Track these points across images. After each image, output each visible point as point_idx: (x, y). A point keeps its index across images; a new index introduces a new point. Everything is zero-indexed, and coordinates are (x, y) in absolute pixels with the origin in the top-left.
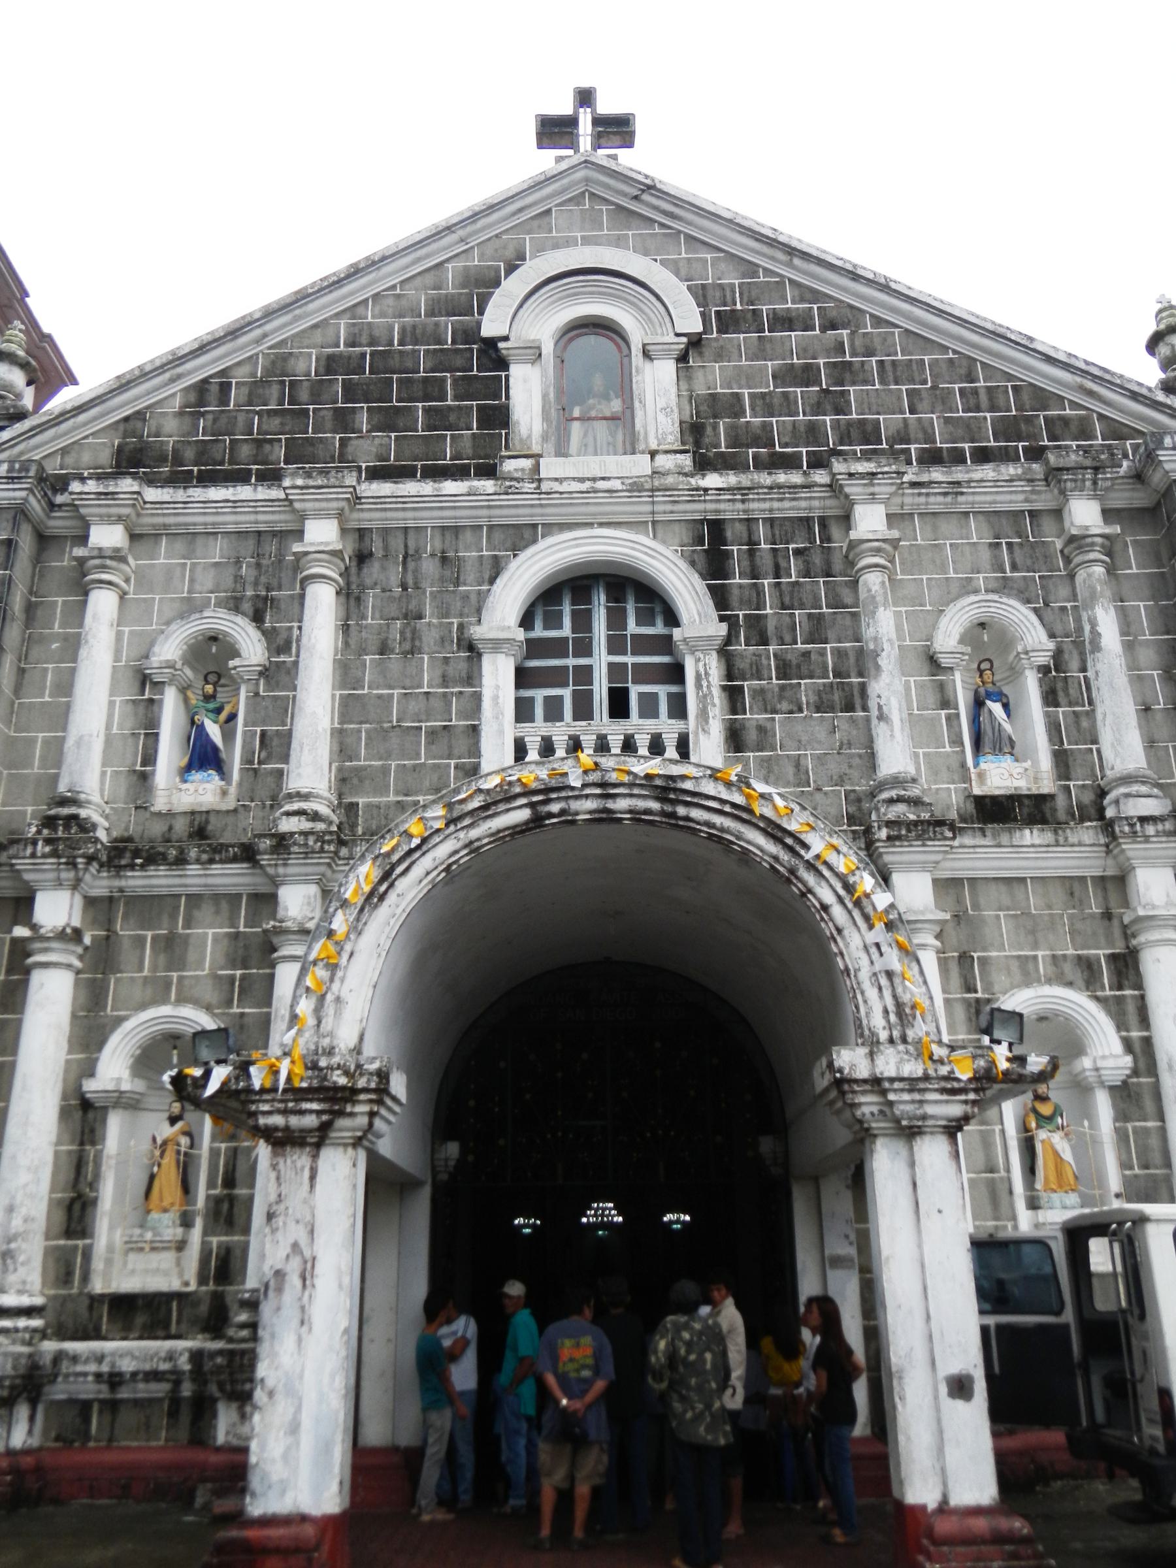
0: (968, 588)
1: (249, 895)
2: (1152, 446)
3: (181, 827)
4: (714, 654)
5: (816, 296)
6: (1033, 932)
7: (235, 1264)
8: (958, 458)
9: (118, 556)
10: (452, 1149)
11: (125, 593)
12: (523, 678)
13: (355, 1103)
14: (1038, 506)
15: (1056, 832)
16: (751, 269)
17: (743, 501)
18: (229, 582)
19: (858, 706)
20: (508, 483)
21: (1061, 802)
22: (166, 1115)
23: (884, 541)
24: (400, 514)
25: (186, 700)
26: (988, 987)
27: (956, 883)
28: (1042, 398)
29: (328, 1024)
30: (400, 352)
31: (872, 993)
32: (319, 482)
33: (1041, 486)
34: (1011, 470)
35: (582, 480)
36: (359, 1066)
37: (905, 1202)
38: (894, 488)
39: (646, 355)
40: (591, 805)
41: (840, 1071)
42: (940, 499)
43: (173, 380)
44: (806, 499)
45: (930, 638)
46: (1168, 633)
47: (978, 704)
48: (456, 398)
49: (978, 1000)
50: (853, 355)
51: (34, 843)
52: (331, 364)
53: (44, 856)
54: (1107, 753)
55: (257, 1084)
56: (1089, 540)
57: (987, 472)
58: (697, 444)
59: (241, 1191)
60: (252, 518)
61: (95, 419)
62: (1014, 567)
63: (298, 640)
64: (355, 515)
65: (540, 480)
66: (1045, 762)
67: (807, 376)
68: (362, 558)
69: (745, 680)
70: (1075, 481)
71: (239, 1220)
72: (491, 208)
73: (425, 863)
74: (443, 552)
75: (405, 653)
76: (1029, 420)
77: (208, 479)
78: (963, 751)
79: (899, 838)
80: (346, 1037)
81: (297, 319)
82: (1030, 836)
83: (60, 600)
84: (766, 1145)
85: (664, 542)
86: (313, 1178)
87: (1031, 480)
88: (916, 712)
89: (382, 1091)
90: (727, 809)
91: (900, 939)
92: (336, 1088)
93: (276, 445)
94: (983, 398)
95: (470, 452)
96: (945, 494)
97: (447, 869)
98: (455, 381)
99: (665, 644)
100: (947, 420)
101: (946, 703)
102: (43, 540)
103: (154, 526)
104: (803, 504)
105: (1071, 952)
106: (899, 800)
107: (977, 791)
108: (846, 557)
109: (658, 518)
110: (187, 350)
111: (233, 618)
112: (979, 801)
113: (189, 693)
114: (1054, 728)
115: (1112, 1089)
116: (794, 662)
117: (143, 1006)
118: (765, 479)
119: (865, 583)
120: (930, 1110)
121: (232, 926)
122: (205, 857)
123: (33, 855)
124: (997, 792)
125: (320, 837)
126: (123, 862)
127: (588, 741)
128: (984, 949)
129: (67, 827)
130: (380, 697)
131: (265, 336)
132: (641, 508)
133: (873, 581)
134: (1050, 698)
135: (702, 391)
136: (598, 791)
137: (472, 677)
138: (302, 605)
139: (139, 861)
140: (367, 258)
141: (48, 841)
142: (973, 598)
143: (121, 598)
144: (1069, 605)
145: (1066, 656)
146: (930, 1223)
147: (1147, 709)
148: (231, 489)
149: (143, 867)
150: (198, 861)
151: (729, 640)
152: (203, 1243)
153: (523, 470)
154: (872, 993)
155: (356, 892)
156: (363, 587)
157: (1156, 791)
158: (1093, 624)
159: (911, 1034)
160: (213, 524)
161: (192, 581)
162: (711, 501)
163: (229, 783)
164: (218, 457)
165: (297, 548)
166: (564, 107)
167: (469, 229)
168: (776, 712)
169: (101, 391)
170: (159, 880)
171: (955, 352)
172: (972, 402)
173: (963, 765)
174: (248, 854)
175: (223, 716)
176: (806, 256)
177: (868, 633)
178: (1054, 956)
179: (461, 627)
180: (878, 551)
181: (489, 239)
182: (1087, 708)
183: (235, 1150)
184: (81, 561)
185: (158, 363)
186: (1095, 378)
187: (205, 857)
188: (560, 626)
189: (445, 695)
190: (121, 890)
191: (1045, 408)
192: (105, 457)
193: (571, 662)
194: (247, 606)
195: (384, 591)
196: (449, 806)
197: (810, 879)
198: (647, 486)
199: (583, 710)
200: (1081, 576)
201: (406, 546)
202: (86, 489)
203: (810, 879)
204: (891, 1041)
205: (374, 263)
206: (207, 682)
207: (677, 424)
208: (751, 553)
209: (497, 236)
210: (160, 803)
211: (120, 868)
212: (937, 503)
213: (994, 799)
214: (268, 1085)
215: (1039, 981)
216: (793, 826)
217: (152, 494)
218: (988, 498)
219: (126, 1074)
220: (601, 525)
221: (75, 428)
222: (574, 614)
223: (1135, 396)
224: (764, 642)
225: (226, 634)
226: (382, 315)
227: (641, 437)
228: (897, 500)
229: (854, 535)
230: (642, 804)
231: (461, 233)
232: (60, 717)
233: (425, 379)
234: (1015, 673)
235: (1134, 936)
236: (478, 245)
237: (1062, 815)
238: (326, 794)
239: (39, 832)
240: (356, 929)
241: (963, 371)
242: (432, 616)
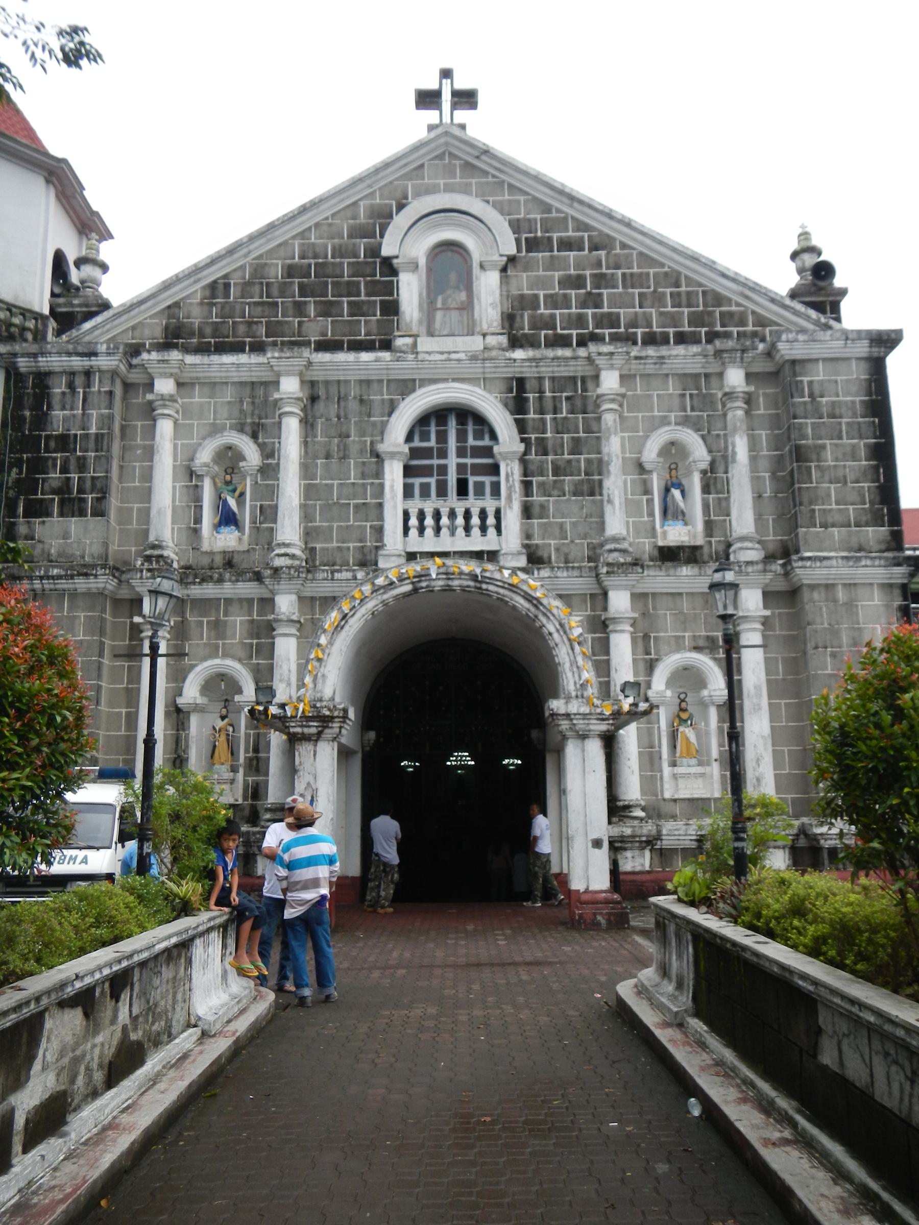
0: (664, 422)
1: (258, 599)
2: (775, 340)
3: (218, 560)
4: (517, 462)
5: (587, 228)
6: (684, 622)
7: (261, 791)
8: (664, 340)
9: (172, 399)
10: (372, 735)
11: (177, 420)
12: (409, 471)
13: (333, 722)
14: (709, 371)
15: (700, 568)
16: (548, 208)
17: (537, 367)
18: (236, 413)
19: (597, 493)
20: (398, 354)
21: (706, 550)
22: (219, 715)
23: (617, 395)
24: (336, 373)
25: (215, 483)
26: (657, 653)
27: (644, 595)
28: (719, 299)
29: (319, 686)
30: (333, 264)
31: (569, 674)
32: (288, 355)
33: (711, 359)
34: (695, 349)
35: (442, 353)
36: (334, 706)
37: (579, 767)
38: (624, 362)
39: (482, 267)
40: (441, 583)
41: (552, 710)
42: (652, 366)
43: (195, 282)
44: (574, 365)
45: (640, 452)
46: (776, 450)
47: (667, 490)
48: (367, 295)
49: (651, 659)
50: (607, 268)
51: (142, 571)
52: (291, 271)
53: (147, 578)
54: (734, 523)
55: (289, 714)
56: (735, 395)
57: (680, 350)
58: (511, 327)
59: (261, 755)
60: (249, 374)
61: (151, 307)
62: (692, 409)
63: (279, 450)
64: (309, 373)
65: (417, 353)
66: (700, 526)
67: (578, 282)
68: (314, 399)
69: (533, 476)
70: (730, 357)
71: (262, 769)
72: (386, 165)
73: (363, 611)
74: (361, 396)
75: (340, 459)
76: (711, 314)
77: (221, 349)
78: (654, 521)
79: (613, 572)
80: (328, 692)
81: (269, 241)
82: (686, 571)
83: (139, 424)
84: (535, 734)
85: (490, 392)
86: (315, 755)
87: (705, 356)
88: (630, 497)
89: (345, 717)
90: (506, 586)
91: (584, 650)
92: (325, 716)
93: (260, 325)
94: (684, 299)
95: (375, 331)
96: (655, 364)
97: (373, 614)
98: (366, 283)
99: (488, 452)
100: (661, 314)
101: (647, 491)
102: (127, 386)
103: (191, 378)
104: (572, 368)
105: (704, 633)
106: (616, 550)
107: (660, 544)
108: (596, 401)
109: (487, 376)
110: (203, 264)
111: (241, 437)
112: (661, 550)
113: (217, 480)
114: (706, 507)
115: (719, 706)
116: (562, 466)
117: (205, 659)
118: (550, 353)
119: (605, 420)
120: (592, 727)
121: (249, 616)
122: (234, 578)
123: (141, 578)
124: (672, 544)
125: (297, 569)
126: (189, 581)
127: (445, 512)
128: (657, 632)
129: (157, 562)
130: (326, 485)
131: (250, 252)
132: (476, 369)
133: (609, 419)
134: (706, 489)
135: (515, 292)
136: (444, 576)
137: (379, 474)
138: (280, 428)
139: (197, 580)
140: (311, 201)
141: (149, 570)
142: (667, 428)
143: (175, 423)
144: (722, 433)
145: (717, 464)
146: (590, 777)
147: (760, 496)
148: (235, 357)
149: (200, 583)
150: (230, 581)
151: (525, 453)
152: (244, 780)
153: (407, 345)
154: (569, 674)
155: (330, 626)
156: (315, 418)
157: (757, 546)
158: (734, 446)
159: (585, 694)
160: (226, 377)
161: (215, 412)
162: (518, 367)
163: (243, 534)
164: (226, 332)
165: (276, 396)
166: (432, 84)
167: (373, 179)
168: (550, 496)
169: (154, 291)
170: (209, 590)
171: (669, 267)
172: (677, 301)
173: (654, 528)
174: (258, 577)
175: (237, 493)
176: (581, 202)
177: (605, 450)
178: (694, 636)
179: (372, 443)
180: (613, 401)
181: (386, 185)
182: (726, 495)
183: (258, 734)
184: (150, 403)
185: (187, 272)
186: (751, 289)
187: (234, 578)
188: (429, 440)
189: (363, 484)
190: (188, 596)
191: (719, 305)
192: (158, 332)
193: (435, 462)
194: (248, 429)
195: (327, 420)
196: (373, 584)
197: (544, 620)
198: (481, 357)
199: (442, 492)
200: (730, 416)
201: (339, 392)
202: (151, 358)
203: (544, 620)
204: (577, 697)
205: (315, 204)
206: (227, 474)
207: (500, 314)
208: (541, 399)
209: (391, 182)
210: (205, 547)
211: (187, 584)
212: (650, 369)
213: (669, 549)
214: (294, 714)
215: (684, 649)
216: (538, 594)
217: (190, 359)
218: (681, 366)
219: (198, 695)
220: (454, 380)
221: (139, 313)
222: (438, 433)
223: (773, 300)
224: (546, 453)
225: (236, 446)
226: (321, 237)
227: (478, 323)
228: (627, 367)
229: (600, 391)
230: (465, 583)
231: (368, 182)
232: (147, 495)
233: (348, 283)
234: (689, 473)
235: (738, 625)
236: (380, 189)
237: (706, 558)
238: (298, 543)
239: (142, 564)
240: (331, 643)
241: (673, 280)
242: (355, 435)
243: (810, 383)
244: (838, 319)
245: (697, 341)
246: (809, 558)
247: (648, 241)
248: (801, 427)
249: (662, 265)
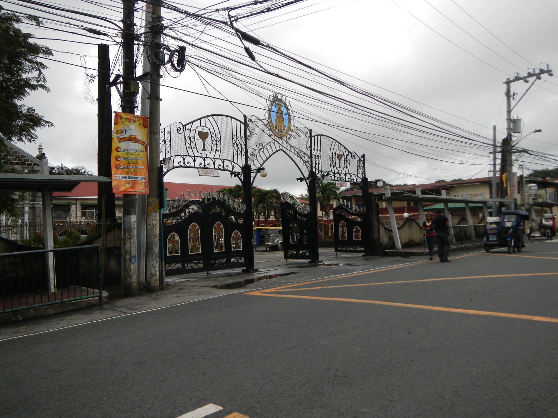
28: (24, 157)
34: (19, 166)
245: (20, 165)
246: (37, 203)
247: (11, 145)
249: (14, 150)
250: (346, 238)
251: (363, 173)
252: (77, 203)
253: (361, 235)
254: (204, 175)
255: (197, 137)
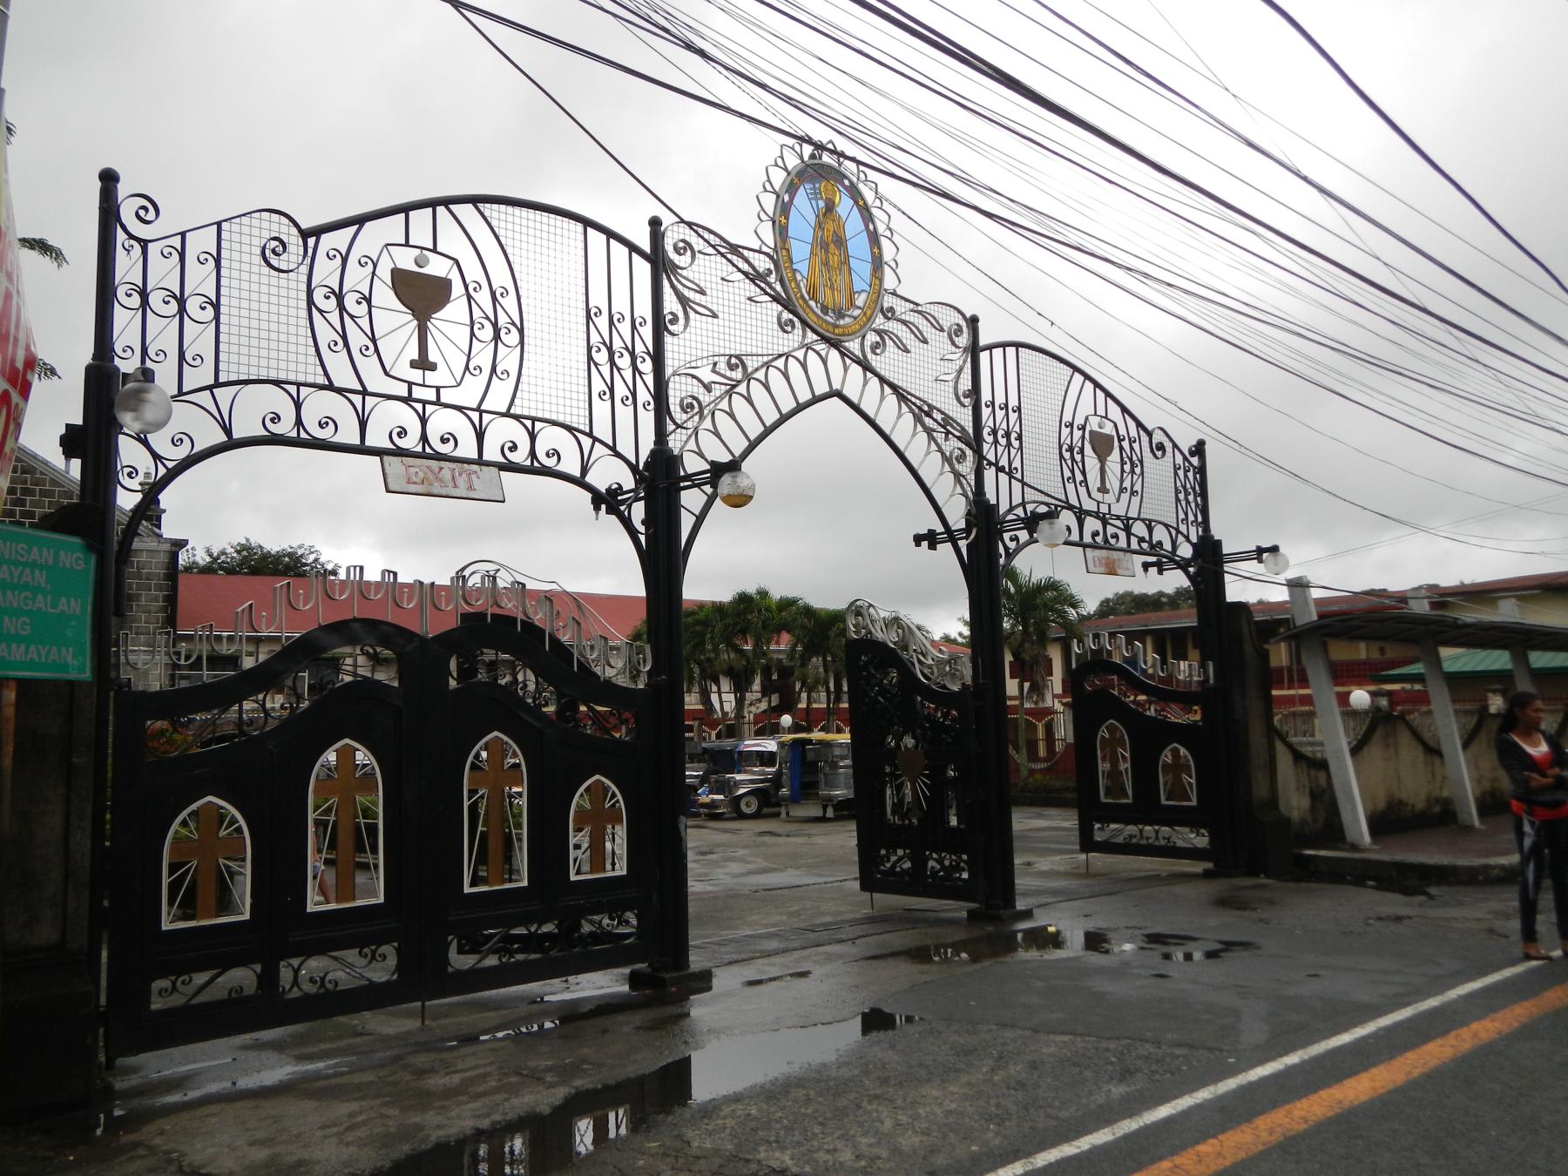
243: (138, 562)
244: (159, 527)
248: (130, 584)
250: (1130, 793)
251: (1200, 519)
252: (261, 650)
253: (1193, 781)
254: (412, 488)
255: (385, 296)
